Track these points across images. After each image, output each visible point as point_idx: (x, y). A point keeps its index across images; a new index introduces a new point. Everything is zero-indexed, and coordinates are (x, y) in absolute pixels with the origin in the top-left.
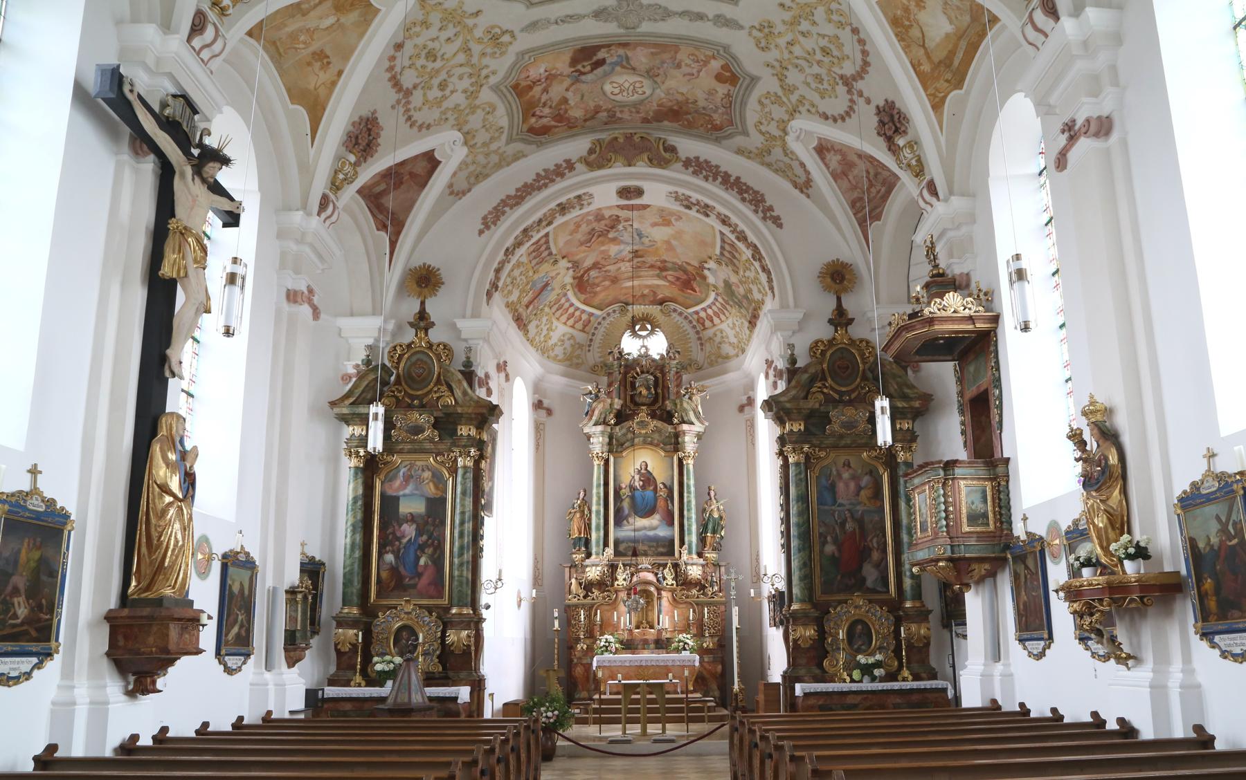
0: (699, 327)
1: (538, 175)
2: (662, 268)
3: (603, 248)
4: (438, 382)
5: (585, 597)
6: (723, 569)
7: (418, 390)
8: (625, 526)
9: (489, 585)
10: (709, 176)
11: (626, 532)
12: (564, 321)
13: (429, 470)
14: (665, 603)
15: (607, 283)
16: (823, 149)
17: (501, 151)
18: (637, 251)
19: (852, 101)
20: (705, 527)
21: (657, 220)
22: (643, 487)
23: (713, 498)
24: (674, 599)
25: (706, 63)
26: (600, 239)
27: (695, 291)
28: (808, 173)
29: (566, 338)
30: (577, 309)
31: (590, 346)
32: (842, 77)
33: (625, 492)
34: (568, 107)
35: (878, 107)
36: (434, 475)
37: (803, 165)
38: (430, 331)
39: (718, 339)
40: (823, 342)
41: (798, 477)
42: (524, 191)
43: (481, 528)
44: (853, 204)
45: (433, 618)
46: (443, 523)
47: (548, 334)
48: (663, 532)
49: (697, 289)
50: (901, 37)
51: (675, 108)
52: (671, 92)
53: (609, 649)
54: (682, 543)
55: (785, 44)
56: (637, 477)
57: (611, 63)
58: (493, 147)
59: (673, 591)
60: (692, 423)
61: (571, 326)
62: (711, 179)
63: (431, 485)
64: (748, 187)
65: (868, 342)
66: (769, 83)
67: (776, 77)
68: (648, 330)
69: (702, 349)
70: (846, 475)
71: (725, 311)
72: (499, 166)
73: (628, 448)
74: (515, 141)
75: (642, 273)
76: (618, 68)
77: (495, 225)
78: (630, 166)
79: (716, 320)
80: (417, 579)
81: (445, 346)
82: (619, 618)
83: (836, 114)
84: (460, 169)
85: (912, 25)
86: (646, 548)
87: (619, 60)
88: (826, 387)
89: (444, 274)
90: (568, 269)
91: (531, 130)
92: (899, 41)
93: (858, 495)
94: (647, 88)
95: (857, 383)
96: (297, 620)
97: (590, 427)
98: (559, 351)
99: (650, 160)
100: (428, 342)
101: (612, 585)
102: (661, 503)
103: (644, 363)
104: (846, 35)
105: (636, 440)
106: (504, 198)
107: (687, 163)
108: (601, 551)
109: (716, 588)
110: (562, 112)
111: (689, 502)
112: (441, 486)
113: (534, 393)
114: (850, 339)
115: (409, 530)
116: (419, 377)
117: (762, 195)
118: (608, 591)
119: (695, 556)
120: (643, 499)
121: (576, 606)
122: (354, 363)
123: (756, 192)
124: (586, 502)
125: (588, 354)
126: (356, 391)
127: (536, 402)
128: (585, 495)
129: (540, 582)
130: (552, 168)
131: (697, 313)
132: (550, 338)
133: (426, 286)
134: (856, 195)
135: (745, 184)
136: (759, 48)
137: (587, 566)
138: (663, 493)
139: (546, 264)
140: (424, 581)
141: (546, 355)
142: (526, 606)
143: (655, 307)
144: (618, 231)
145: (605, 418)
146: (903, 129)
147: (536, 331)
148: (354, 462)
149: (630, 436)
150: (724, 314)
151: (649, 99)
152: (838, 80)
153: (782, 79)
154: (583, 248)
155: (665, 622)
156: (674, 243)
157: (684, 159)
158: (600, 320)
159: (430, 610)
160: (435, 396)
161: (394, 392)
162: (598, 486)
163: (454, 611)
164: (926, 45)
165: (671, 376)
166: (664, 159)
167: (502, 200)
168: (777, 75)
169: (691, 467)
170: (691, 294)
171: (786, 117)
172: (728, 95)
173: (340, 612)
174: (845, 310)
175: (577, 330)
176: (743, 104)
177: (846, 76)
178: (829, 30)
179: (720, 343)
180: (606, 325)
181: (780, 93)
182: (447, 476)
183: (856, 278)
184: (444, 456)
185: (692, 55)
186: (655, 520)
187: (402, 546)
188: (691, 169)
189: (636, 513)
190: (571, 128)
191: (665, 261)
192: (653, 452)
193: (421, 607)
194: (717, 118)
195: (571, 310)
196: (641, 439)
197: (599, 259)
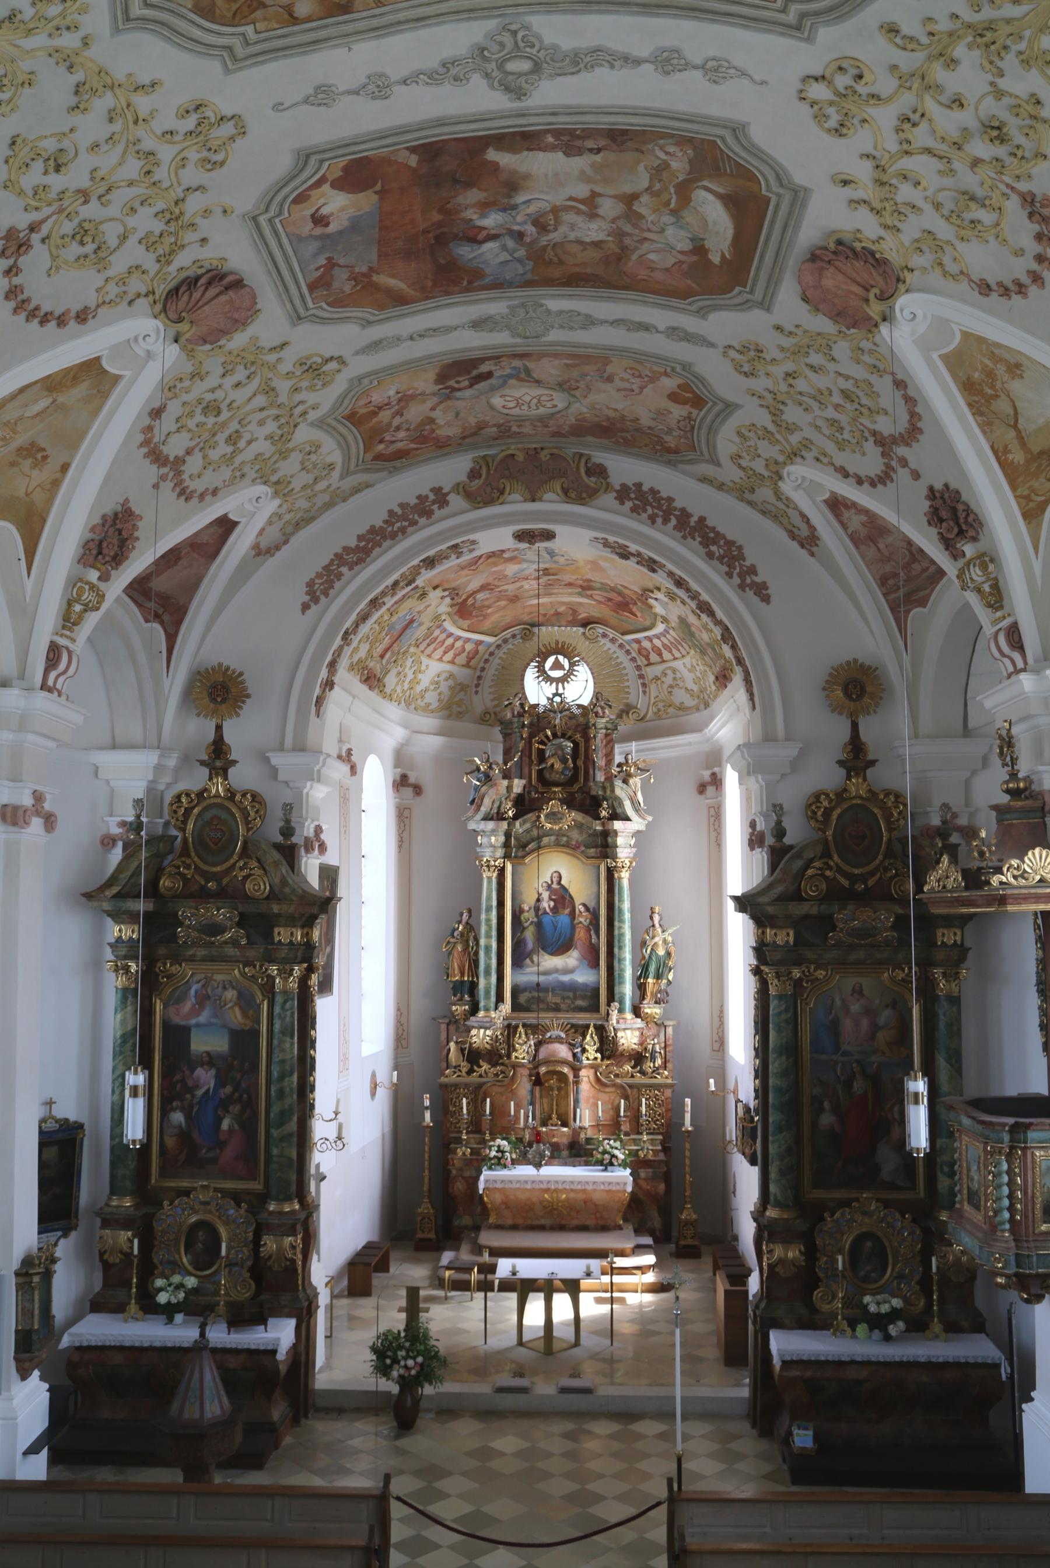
0: (641, 661)
1: (391, 513)
2: (586, 587)
4: (245, 853)
5: (470, 1072)
6: (670, 1030)
7: (215, 865)
8: (528, 966)
9: (324, 1146)
10: (657, 516)
11: (529, 976)
12: (438, 657)
13: (233, 988)
14: (585, 1087)
15: (503, 603)
16: (836, 505)
17: (332, 489)
18: (547, 569)
19: (888, 466)
20: (645, 969)
22: (555, 910)
23: (657, 925)
24: (598, 1080)
25: (653, 379)
27: (636, 616)
28: (812, 529)
29: (441, 679)
30: (459, 638)
31: (477, 686)
32: (874, 433)
33: (528, 916)
34: (434, 427)
35: (931, 489)
36: (240, 995)
37: (803, 516)
38: (231, 771)
39: (668, 680)
40: (827, 795)
41: (784, 1017)
42: (369, 541)
43: (311, 1075)
44: (883, 581)
45: (242, 1211)
46: (255, 1068)
48: (583, 977)
49: (639, 614)
50: (976, 410)
51: (604, 423)
52: (597, 406)
53: (502, 1161)
54: (611, 998)
55: (783, 375)
56: (546, 895)
57: (502, 376)
58: (321, 486)
59: (595, 1067)
60: (628, 819)
61: (449, 662)
62: (659, 520)
63: (237, 1010)
64: (717, 533)
65: (897, 796)
66: (751, 413)
67: (765, 411)
68: (561, 667)
69: (644, 692)
70: (855, 1008)
72: (329, 505)
73: (532, 851)
74: (355, 472)
75: (555, 591)
76: (514, 382)
77: (326, 595)
78: (533, 500)
79: (666, 655)
80: (218, 1151)
81: (254, 796)
82: (517, 1111)
83: (862, 474)
84: (270, 522)
85: (997, 396)
86: (558, 1000)
87: (514, 372)
88: (830, 868)
89: (251, 683)
90: (442, 598)
91: (378, 457)
92: (973, 414)
93: (872, 1037)
94: (560, 400)
95: (877, 862)
96: (33, 1314)
97: (478, 822)
98: (432, 698)
99: (566, 492)
100: (228, 790)
101: (509, 1056)
102: (580, 934)
103: (557, 721)
104: (884, 385)
106: (340, 551)
107: (623, 494)
108: (493, 1005)
109: (659, 1062)
110: (426, 433)
112: (251, 1012)
113: (396, 766)
114: (870, 791)
115: (206, 1078)
116: (216, 844)
117: (740, 548)
118: (502, 1064)
119: (629, 1016)
120: (555, 927)
121: (456, 1086)
122: (119, 819)
123: (730, 543)
124: (471, 928)
126: (122, 876)
127: (398, 779)
128: (470, 917)
129: (404, 1042)
130: (413, 501)
131: (638, 641)
133: (224, 701)
134: (888, 568)
135: (713, 529)
136: (741, 372)
138: (583, 919)
140: (229, 1153)
141: (413, 706)
142: (383, 1095)
145: (499, 807)
146: (971, 533)
147: (395, 680)
148: (121, 981)
149: (535, 833)
151: (564, 413)
152: (867, 434)
153: (776, 415)
154: (466, 572)
155: (586, 1116)
157: (618, 488)
158: (492, 649)
159: (236, 1197)
160: (241, 875)
161: (179, 867)
162: (489, 909)
163: (272, 1208)
164: (1020, 426)
165: (599, 741)
166: (588, 487)
167: (336, 555)
168: (768, 407)
171: (781, 458)
172: (689, 418)
173: (107, 1205)
174: (864, 744)
176: (712, 431)
177: (881, 434)
178: (859, 372)
179: (671, 686)
180: (501, 654)
181: (771, 427)
182: (261, 998)
183: (883, 690)
184: (255, 967)
185: (631, 369)
186: (571, 959)
187: (195, 1101)
188: (629, 504)
190: (441, 447)
192: (569, 857)
193: (225, 1193)
194: (671, 441)
196: (553, 838)
197: (490, 580)
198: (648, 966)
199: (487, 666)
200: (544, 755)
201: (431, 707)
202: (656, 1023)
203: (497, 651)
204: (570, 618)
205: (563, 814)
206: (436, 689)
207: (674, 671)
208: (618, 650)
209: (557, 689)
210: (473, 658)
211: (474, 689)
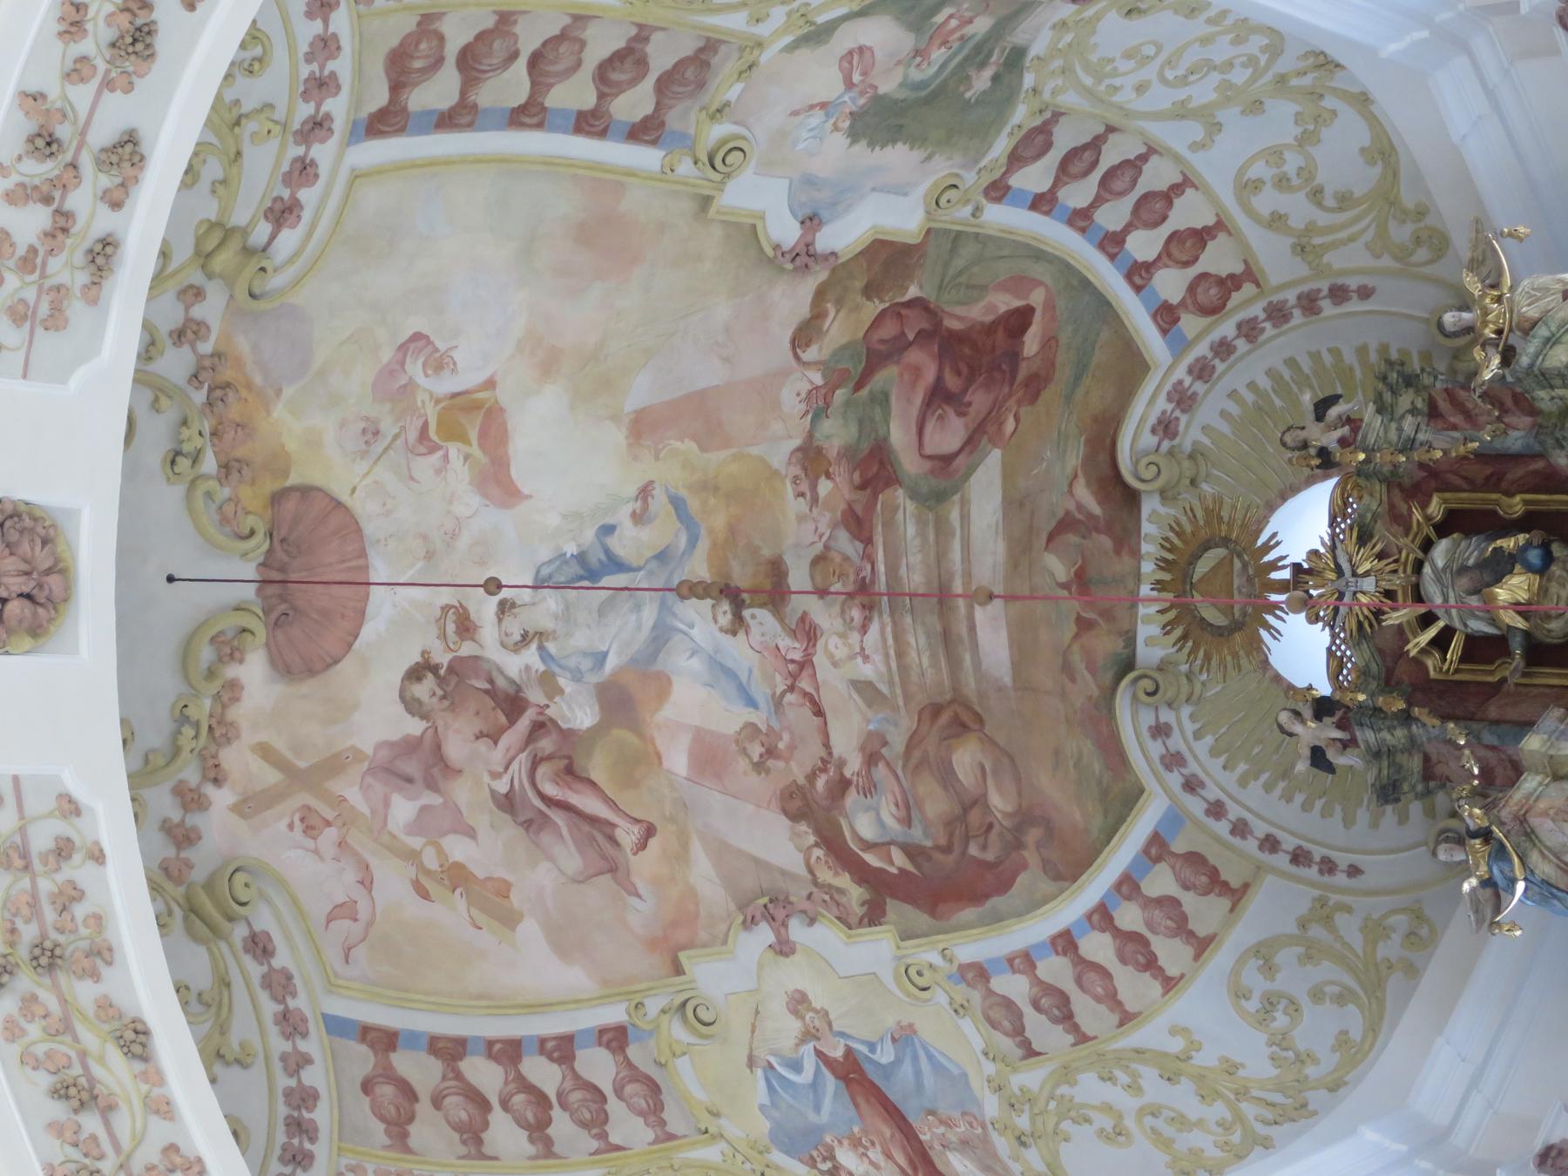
0: (1246, 305)
3: (678, 761)
12: (1156, 988)
21: (459, 473)
26: (598, 774)
30: (1102, 916)
31: (1328, 866)
39: (1299, 209)
47: (1200, 1078)
49: (1005, 302)
61: (1197, 957)
69: (1365, 293)
71: (1110, 157)
79: (1188, 213)
131: (1166, 316)
132: (1231, 1068)
139: (683, 1064)
143: (1147, 528)
144: (547, 681)
150: (1135, 165)
154: (645, 866)
156: (641, 392)
158: (1196, 806)
170: (1049, 342)
179: (1316, 194)
180: (1230, 779)
191: (811, 458)
195: (1098, 946)
200: (1487, 638)
201: (1356, 1034)
203: (1212, 793)
204: (1105, 541)
206: (1294, 1007)
207: (1247, 187)
208: (1223, 386)
209: (1282, 587)
210: (1214, 874)
211: (1341, 879)
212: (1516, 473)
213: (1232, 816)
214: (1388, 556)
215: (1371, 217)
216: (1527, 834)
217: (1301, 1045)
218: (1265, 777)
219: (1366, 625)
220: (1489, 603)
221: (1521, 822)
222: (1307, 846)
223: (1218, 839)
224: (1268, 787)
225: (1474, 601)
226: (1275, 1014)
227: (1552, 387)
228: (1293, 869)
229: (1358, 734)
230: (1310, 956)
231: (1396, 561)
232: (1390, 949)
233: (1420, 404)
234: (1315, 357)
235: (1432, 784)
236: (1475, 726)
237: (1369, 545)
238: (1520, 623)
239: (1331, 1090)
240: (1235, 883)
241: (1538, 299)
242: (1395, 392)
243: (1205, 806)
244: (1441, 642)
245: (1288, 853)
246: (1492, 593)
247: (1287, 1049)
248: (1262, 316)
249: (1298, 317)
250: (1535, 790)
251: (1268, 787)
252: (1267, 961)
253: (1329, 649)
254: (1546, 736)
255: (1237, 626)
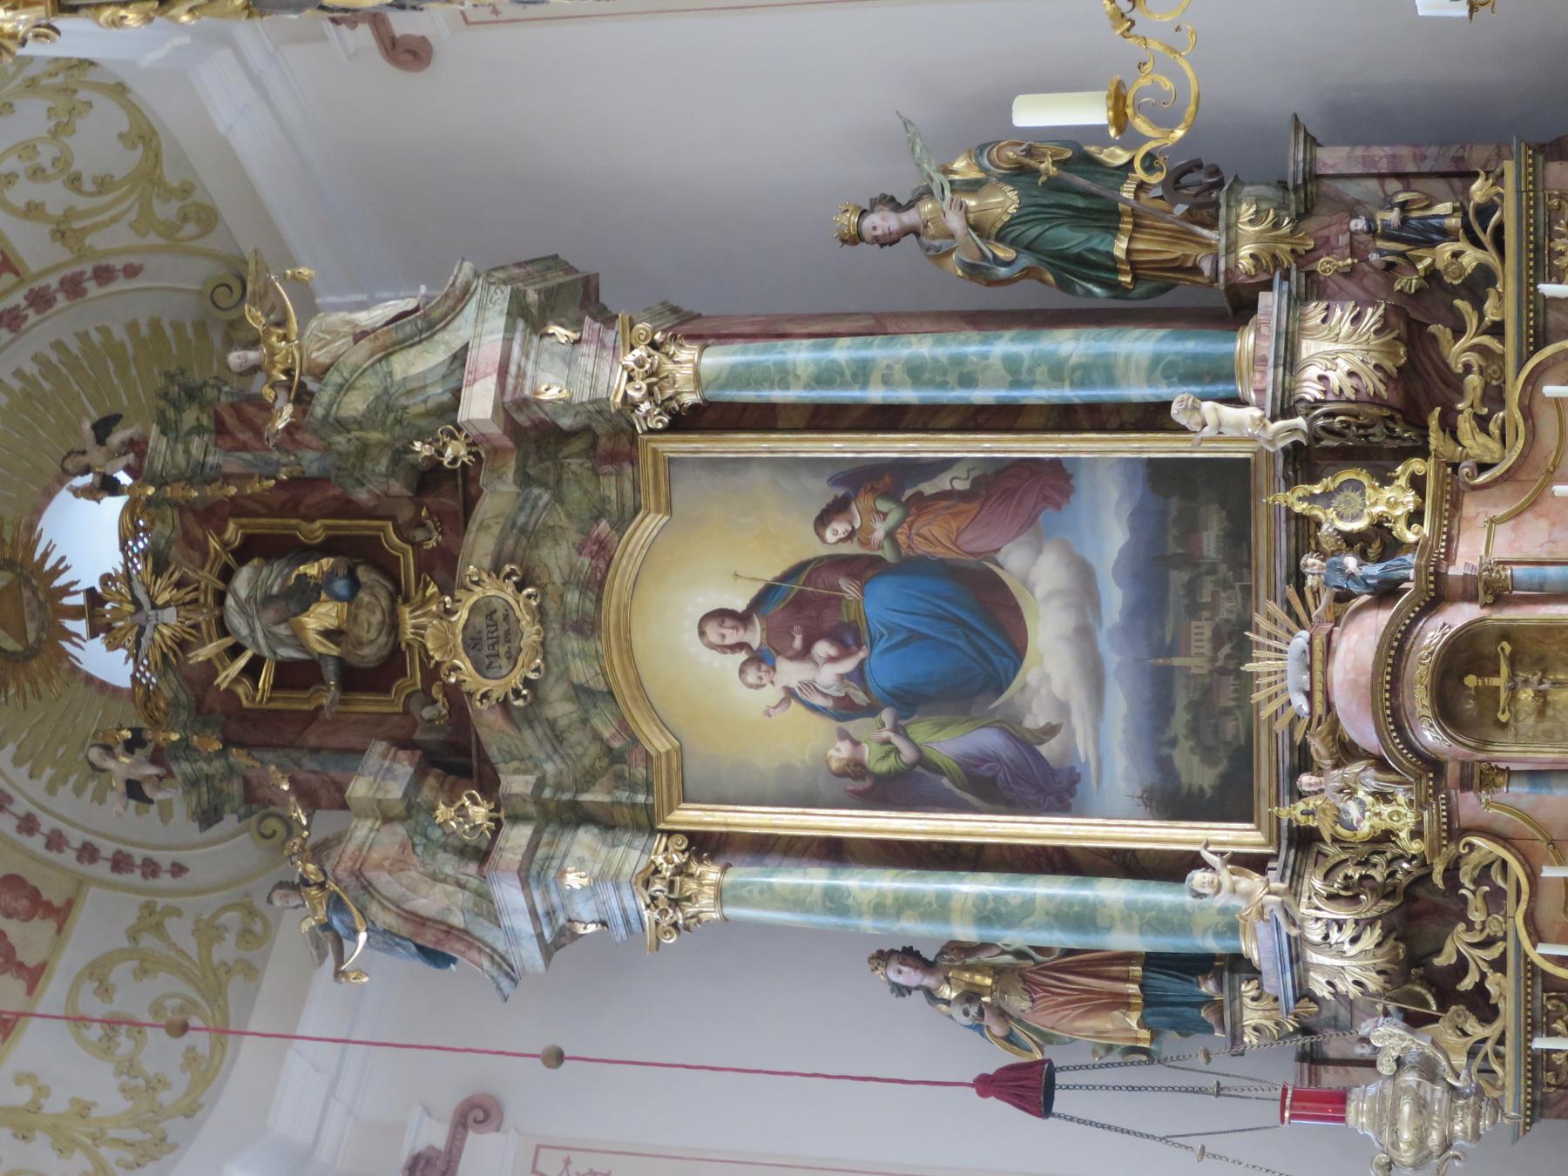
6: (1332, 158)
8: (1070, 749)
22: (846, 638)
23: (909, 218)
31: (151, 869)
39: (56, 197)
47: (54, 1129)
56: (790, 673)
60: (460, 358)
61: (31, 990)
69: (132, 271)
73: (624, 726)
86: (1202, 630)
97: (513, 937)
103: (170, 615)
105: (581, 672)
111: (916, 373)
118: (1452, 872)
120: (913, 637)
125: (197, 875)
132: (83, 1109)
137: (1303, 993)
169: (718, 359)
175: (56, 948)
179: (74, 182)
180: (37, 789)
189: (998, 682)
196: (573, 643)
198: (1063, 256)
199: (76, 838)
202: (1299, 218)
205: (472, 610)
209: (76, 613)
210: (34, 895)
211: (165, 880)
212: (312, 499)
213: (45, 829)
214: (188, 585)
215: (132, 199)
216: (364, 888)
217: (150, 1068)
218: (73, 779)
219: (171, 655)
220: (297, 638)
221: (357, 878)
222: (126, 849)
223: (34, 857)
224: (78, 791)
225: (282, 630)
226: (118, 1040)
227: (349, 431)
228: (115, 877)
229: (175, 768)
230: (143, 972)
231: (196, 589)
232: (228, 950)
233: (205, 421)
234: (83, 337)
235: (254, 807)
236: (295, 754)
237: (166, 575)
238: (333, 650)
239: (187, 1116)
240: (57, 901)
241: (328, 344)
242: (178, 409)
243: (15, 822)
244: (252, 670)
245: (107, 860)
246: (300, 622)
247: (136, 1077)
248: (24, 304)
249: (61, 301)
250: (367, 837)
251: (78, 791)
252: (101, 982)
253: (133, 677)
254: (372, 778)
255: (31, 653)
